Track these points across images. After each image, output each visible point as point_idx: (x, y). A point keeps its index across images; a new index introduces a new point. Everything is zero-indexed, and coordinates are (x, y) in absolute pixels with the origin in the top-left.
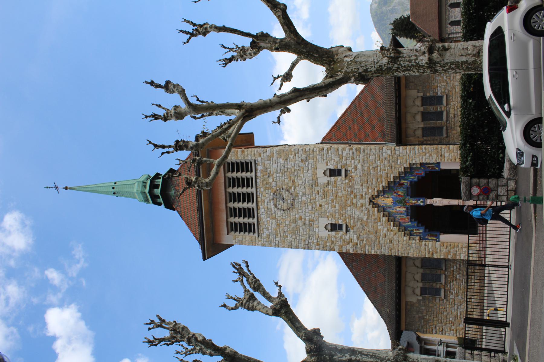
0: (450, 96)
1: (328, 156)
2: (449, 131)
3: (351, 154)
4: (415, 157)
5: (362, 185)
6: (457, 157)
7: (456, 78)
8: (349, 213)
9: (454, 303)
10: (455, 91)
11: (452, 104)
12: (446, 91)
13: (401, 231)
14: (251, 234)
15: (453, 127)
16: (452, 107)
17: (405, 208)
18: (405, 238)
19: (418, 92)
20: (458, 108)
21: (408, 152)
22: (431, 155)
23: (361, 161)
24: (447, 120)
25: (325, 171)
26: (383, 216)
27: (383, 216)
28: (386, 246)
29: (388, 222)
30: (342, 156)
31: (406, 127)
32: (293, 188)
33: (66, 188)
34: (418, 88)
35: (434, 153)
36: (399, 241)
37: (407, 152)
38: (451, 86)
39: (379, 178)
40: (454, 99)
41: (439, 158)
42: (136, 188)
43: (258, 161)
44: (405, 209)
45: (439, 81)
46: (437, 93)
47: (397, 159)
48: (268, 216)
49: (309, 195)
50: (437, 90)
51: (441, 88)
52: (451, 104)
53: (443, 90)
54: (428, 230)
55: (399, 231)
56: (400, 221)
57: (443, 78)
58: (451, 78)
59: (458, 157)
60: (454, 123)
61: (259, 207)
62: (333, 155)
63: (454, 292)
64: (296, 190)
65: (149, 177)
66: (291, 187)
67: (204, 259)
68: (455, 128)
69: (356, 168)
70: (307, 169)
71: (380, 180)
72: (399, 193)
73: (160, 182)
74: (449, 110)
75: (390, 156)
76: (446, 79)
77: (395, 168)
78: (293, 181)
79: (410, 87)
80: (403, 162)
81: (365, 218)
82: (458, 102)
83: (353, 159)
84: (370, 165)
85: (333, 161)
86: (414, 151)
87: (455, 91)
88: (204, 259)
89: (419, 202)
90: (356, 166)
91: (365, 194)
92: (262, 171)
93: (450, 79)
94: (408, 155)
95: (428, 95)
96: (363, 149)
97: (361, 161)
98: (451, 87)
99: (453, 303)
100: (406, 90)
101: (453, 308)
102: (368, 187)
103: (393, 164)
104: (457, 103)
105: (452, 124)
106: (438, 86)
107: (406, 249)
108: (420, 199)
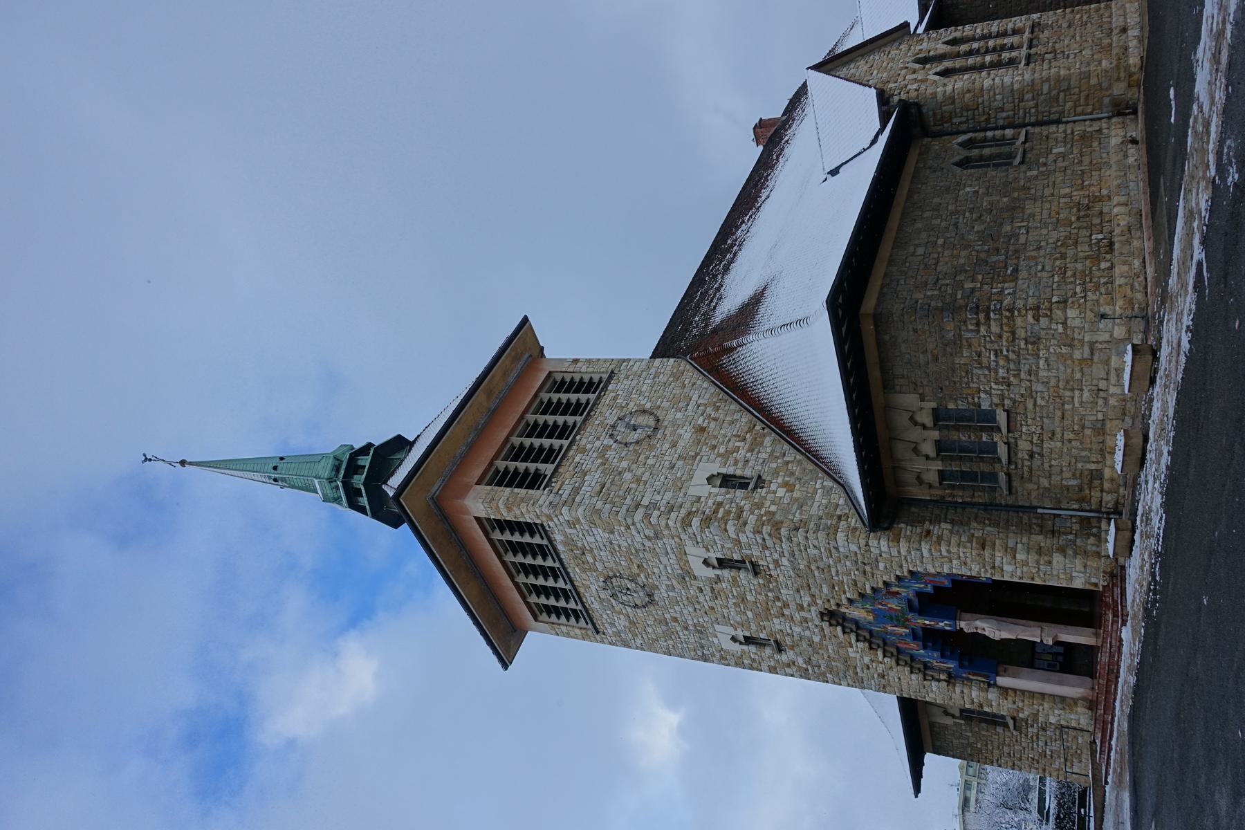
0: (1020, 414)
1: (705, 538)
2: (1014, 484)
3: (760, 541)
4: (922, 562)
5: (798, 591)
6: (1036, 575)
7: (1037, 374)
8: (778, 627)
9: (1038, 738)
10: (1035, 404)
11: (1024, 430)
12: (1007, 402)
13: (903, 664)
14: (582, 623)
15: (1026, 475)
16: (1024, 437)
17: (906, 628)
18: (914, 677)
19: (922, 400)
20: (1042, 441)
21: (903, 552)
22: (966, 564)
23: (786, 554)
24: (1010, 462)
25: (713, 476)
26: (858, 640)
27: (858, 640)
28: (873, 681)
29: (871, 648)
30: (739, 541)
31: (894, 467)
32: (642, 576)
33: (183, 463)
34: (921, 391)
35: (972, 561)
36: (899, 679)
37: (899, 552)
38: (1023, 391)
39: (835, 585)
40: (1030, 422)
41: (986, 571)
42: (325, 469)
43: (549, 527)
44: (908, 631)
45: (982, 378)
46: (979, 405)
47: (877, 560)
48: (606, 608)
49: (683, 591)
50: (979, 398)
51: (990, 394)
52: (1021, 431)
53: (996, 400)
54: (966, 663)
55: (898, 664)
56: (899, 645)
57: (996, 372)
58: (1023, 375)
59: (1039, 576)
60: (1031, 470)
61: (582, 595)
62: (716, 537)
63: (1035, 725)
64: (650, 580)
65: (337, 463)
66: (639, 575)
67: (505, 666)
68: (1035, 479)
69: (778, 562)
70: (664, 551)
71: (839, 588)
72: (889, 606)
73: (366, 461)
74: (1016, 442)
75: (856, 552)
76: (1005, 375)
77: (873, 574)
78: (638, 567)
79: (898, 388)
80: (892, 566)
81: (816, 639)
82: (1042, 428)
83: (765, 547)
84: (809, 563)
85: (719, 547)
86: (918, 553)
87: (1035, 404)
88: (505, 666)
89: (941, 624)
90: (778, 560)
91: (809, 605)
92: (566, 544)
93: (1017, 376)
94: (903, 558)
95: (951, 406)
96: (787, 536)
97: (786, 554)
98: (1022, 395)
99: (1035, 738)
100: (884, 393)
101: (1035, 744)
102: (814, 596)
103: (868, 568)
104: (1039, 428)
105: (1025, 473)
106: (980, 389)
107: (918, 691)
108: (942, 620)
